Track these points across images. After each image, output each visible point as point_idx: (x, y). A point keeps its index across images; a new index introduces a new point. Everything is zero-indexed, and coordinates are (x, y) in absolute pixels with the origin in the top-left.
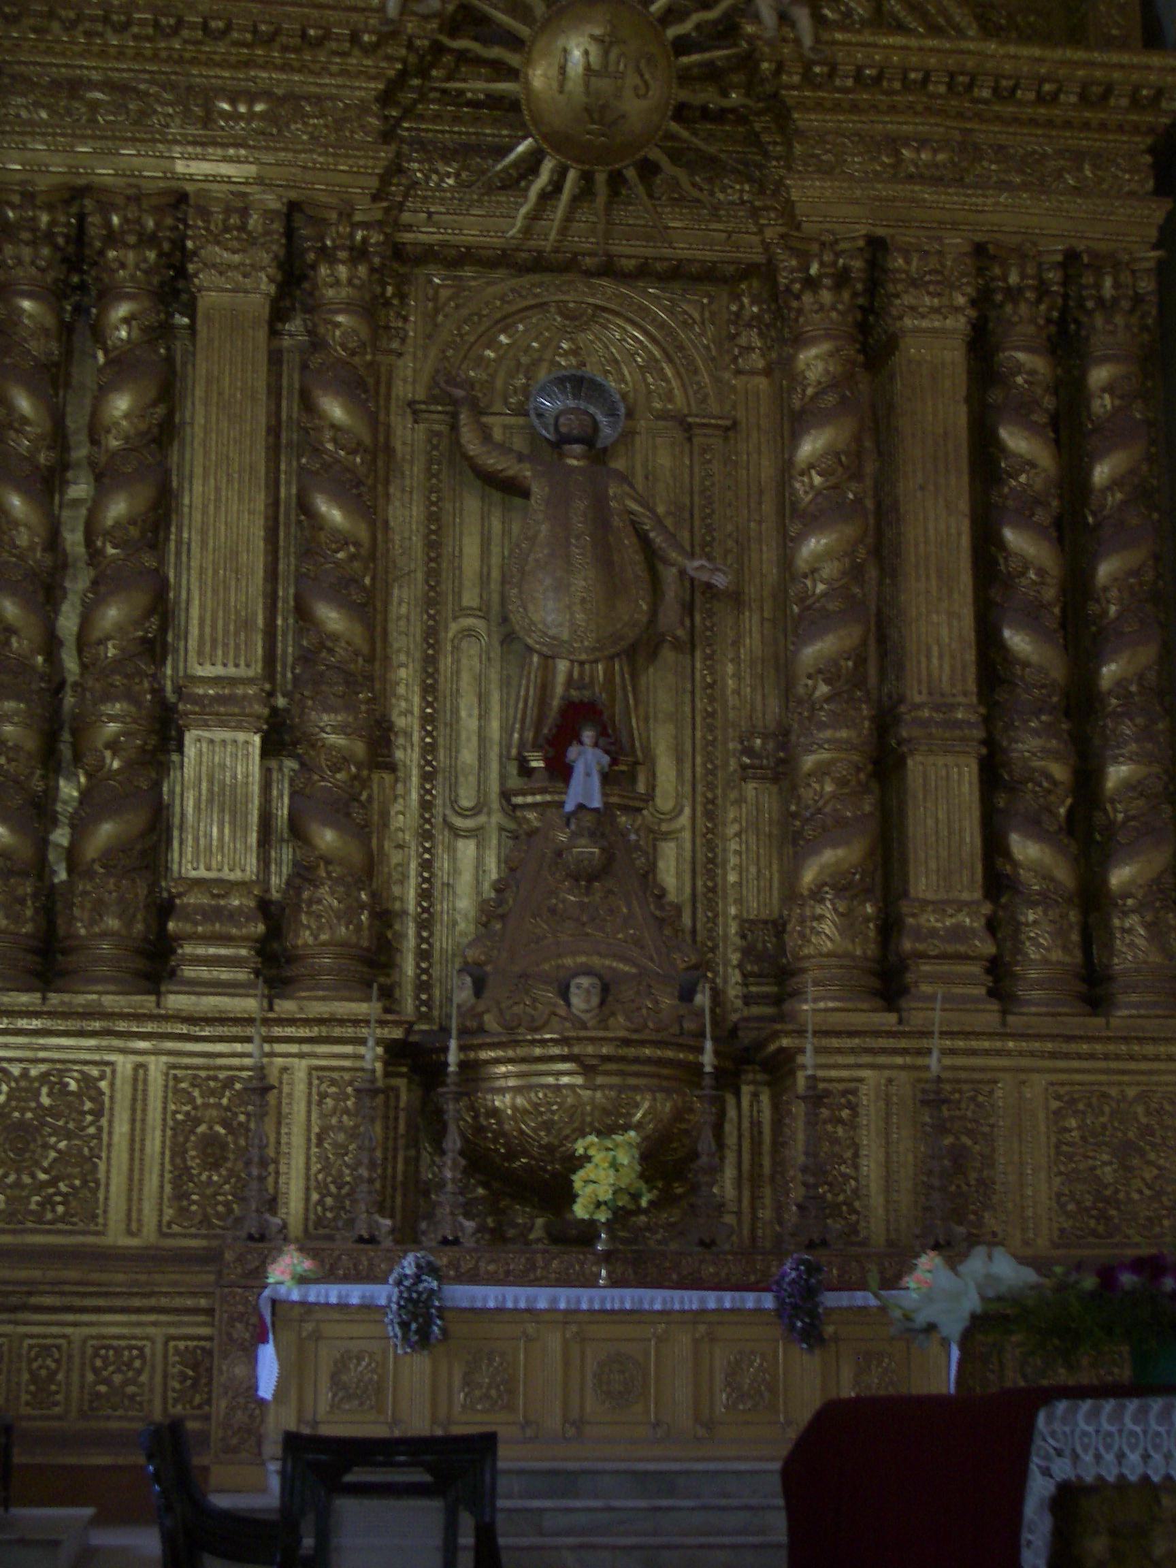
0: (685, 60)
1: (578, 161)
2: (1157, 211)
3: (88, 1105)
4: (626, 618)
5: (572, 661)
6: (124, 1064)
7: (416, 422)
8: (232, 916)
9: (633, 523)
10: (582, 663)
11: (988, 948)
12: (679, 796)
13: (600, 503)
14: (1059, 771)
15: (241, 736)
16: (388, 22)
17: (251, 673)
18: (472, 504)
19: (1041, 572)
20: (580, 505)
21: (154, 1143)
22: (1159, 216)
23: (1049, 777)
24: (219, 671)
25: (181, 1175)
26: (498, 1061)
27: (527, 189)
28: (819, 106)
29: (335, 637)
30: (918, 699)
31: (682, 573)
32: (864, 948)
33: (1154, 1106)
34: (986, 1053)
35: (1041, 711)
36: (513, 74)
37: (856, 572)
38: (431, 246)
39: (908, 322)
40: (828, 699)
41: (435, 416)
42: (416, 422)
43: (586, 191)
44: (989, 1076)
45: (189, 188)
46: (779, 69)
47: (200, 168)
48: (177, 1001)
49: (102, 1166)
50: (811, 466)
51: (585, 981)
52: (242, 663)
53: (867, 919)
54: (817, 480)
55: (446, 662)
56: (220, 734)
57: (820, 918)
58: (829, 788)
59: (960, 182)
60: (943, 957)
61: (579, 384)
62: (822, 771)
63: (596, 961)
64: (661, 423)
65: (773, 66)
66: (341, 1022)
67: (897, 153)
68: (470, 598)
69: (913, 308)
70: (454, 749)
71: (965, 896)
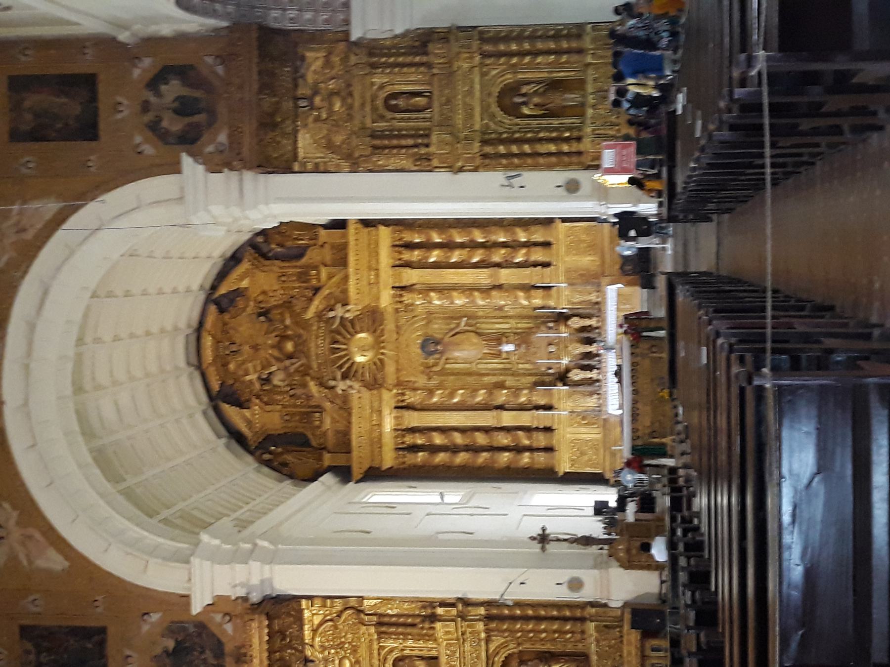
2: (382, 228)
6: (568, 436)
11: (539, 268)
14: (503, 251)
18: (447, 366)
21: (583, 430)
23: (504, 254)
31: (464, 326)
43: (383, 348)
59: (377, 270)
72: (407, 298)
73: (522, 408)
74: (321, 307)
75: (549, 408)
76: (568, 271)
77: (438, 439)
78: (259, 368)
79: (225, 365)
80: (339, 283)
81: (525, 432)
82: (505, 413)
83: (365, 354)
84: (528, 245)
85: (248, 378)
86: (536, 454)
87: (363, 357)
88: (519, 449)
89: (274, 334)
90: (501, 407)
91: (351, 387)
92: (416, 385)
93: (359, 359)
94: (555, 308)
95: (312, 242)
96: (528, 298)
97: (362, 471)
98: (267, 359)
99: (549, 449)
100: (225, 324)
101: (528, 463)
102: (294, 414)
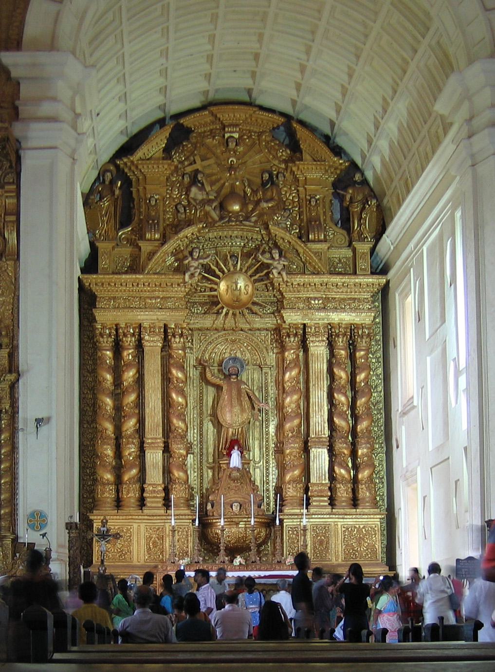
3: (128, 535)
8: (157, 492)
9: (247, 394)
11: (329, 494)
12: (260, 457)
13: (239, 391)
15: (158, 451)
17: (159, 437)
19: (343, 404)
20: (234, 392)
22: (373, 314)
23: (344, 453)
24: (152, 436)
25: (149, 549)
26: (217, 522)
29: (178, 427)
32: (300, 494)
33: (367, 529)
34: (328, 518)
35: (342, 438)
36: (215, 290)
37: (299, 406)
39: (311, 344)
40: (291, 437)
43: (234, 315)
44: (328, 523)
45: (141, 322)
46: (279, 284)
47: (142, 317)
48: (146, 511)
49: (132, 547)
50: (288, 381)
51: (236, 504)
53: (300, 488)
55: (205, 428)
56: (152, 451)
57: (289, 488)
58: (292, 457)
60: (318, 496)
61: (235, 359)
62: (290, 454)
63: (239, 499)
64: (256, 367)
66: (182, 515)
69: (312, 341)
70: (207, 449)
71: (324, 482)
72: (293, 342)
73: (167, 471)
74: (280, 242)
75: (167, 503)
76: (326, 528)
77: (130, 375)
78: (207, 171)
79: (212, 134)
80: (310, 263)
81: (137, 474)
82: (160, 454)
83: (229, 291)
84: (355, 481)
85: (198, 159)
86: (113, 487)
87: (225, 287)
88: (118, 470)
89: (249, 190)
90: (167, 449)
91: (192, 275)
92: (188, 350)
93: (223, 286)
94: (281, 511)
95: (355, 235)
96: (294, 481)
97: (94, 288)
98: (218, 180)
99: (119, 503)
100: (260, 134)
101: (102, 478)
102: (157, 211)
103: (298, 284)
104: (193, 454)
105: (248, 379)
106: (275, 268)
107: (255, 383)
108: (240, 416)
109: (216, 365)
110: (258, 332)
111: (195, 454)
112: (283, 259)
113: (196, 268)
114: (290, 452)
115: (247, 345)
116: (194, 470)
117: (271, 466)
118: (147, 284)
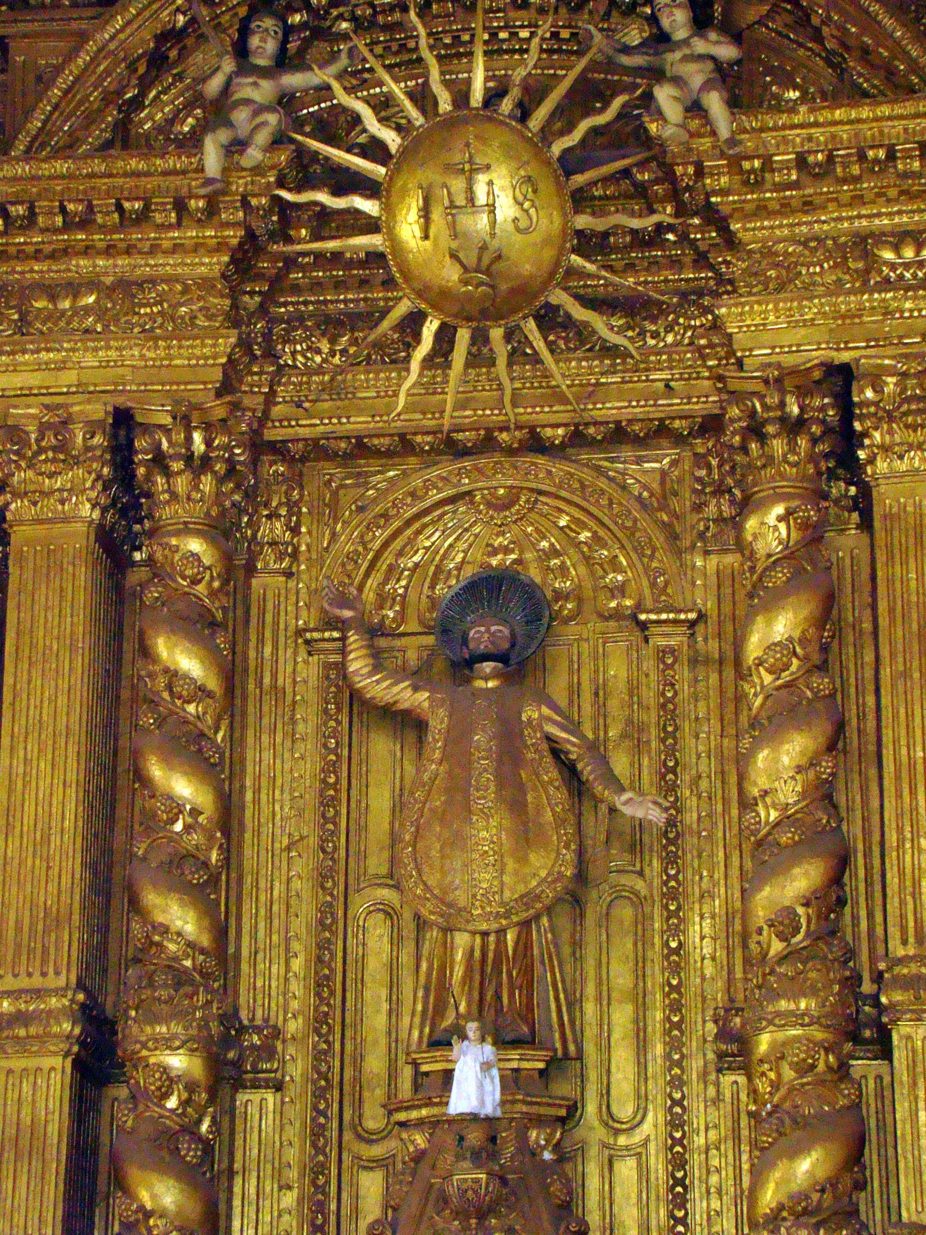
0: (579, 179)
1: (469, 319)
4: (543, 873)
5: (473, 933)
7: (310, 654)
10: (485, 934)
15: (47, 1062)
16: (209, 181)
24: (24, 982)
27: (407, 360)
28: (762, 210)
30: (901, 952)
38: (316, 441)
39: (882, 465)
40: (782, 959)
41: (326, 645)
42: (310, 654)
50: (760, 662)
52: (51, 971)
54: (768, 678)
58: (789, 1074)
62: (778, 1056)
64: (612, 624)
65: (691, 170)
67: (868, 256)
68: (377, 864)
80: (865, 51)
83: (437, 215)
103: (801, 162)
104: (279, 1087)
105: (574, 691)
106: (677, 81)
107: (614, 704)
108: (511, 865)
109: (413, 626)
110: (627, 452)
111: (291, 1091)
112: (713, 36)
113: (260, 109)
114: (773, 1045)
115: (574, 520)
116: (278, 1174)
117: (700, 1141)
118: (21, 210)
